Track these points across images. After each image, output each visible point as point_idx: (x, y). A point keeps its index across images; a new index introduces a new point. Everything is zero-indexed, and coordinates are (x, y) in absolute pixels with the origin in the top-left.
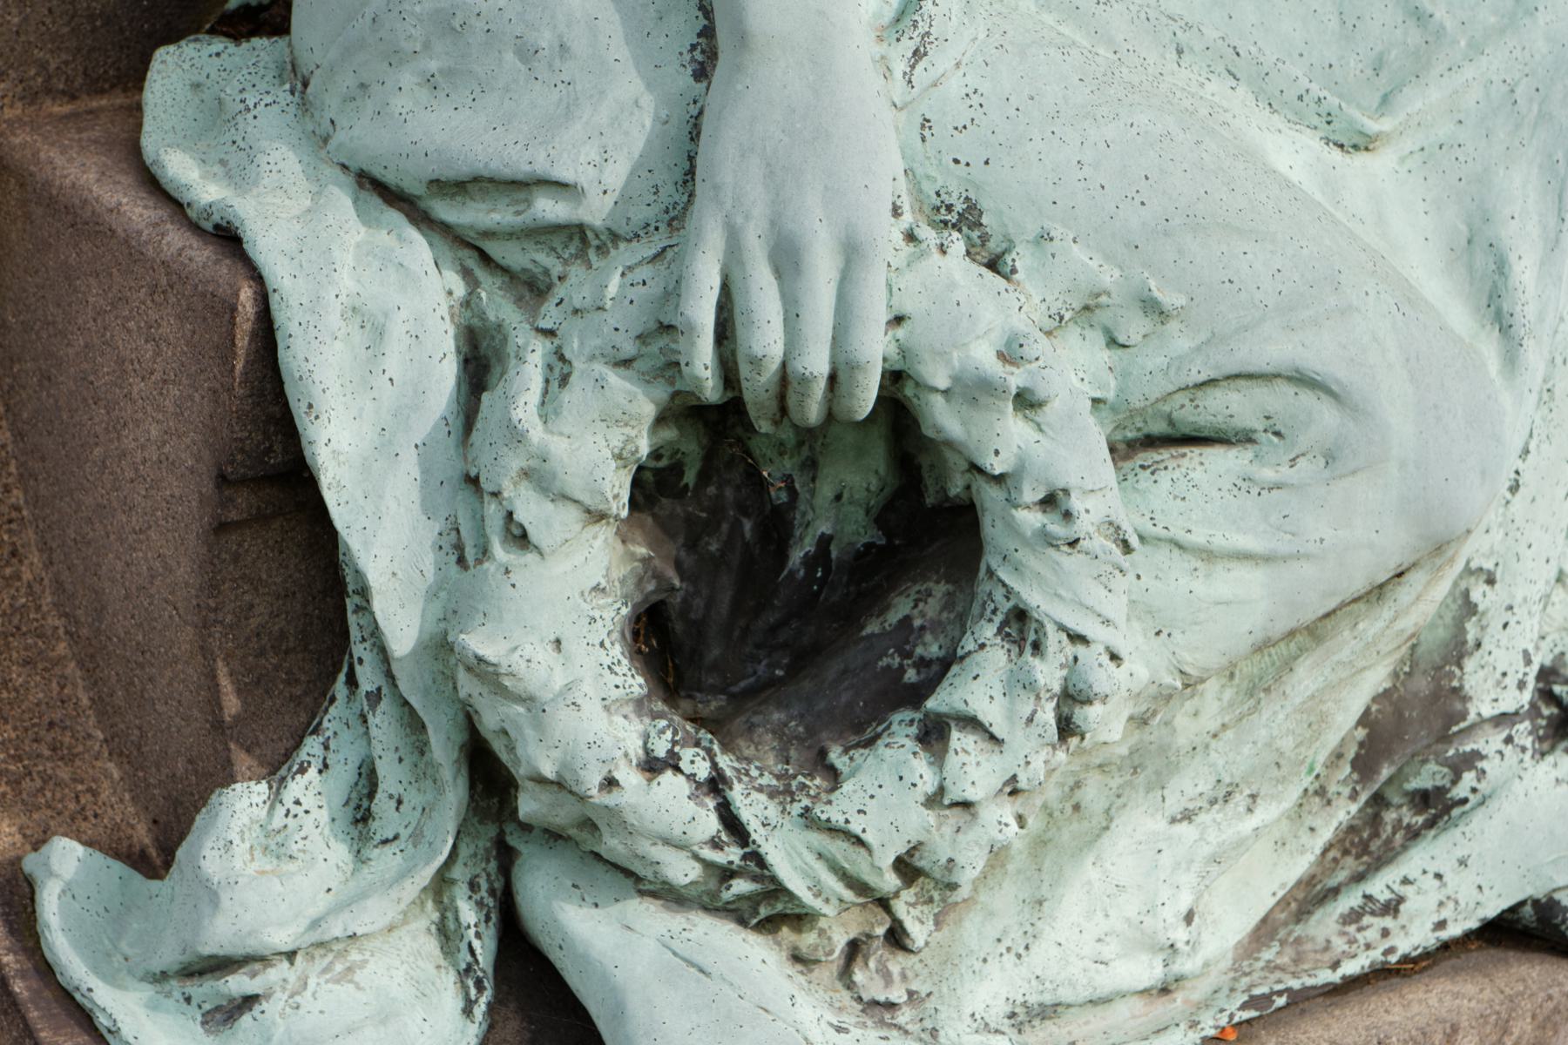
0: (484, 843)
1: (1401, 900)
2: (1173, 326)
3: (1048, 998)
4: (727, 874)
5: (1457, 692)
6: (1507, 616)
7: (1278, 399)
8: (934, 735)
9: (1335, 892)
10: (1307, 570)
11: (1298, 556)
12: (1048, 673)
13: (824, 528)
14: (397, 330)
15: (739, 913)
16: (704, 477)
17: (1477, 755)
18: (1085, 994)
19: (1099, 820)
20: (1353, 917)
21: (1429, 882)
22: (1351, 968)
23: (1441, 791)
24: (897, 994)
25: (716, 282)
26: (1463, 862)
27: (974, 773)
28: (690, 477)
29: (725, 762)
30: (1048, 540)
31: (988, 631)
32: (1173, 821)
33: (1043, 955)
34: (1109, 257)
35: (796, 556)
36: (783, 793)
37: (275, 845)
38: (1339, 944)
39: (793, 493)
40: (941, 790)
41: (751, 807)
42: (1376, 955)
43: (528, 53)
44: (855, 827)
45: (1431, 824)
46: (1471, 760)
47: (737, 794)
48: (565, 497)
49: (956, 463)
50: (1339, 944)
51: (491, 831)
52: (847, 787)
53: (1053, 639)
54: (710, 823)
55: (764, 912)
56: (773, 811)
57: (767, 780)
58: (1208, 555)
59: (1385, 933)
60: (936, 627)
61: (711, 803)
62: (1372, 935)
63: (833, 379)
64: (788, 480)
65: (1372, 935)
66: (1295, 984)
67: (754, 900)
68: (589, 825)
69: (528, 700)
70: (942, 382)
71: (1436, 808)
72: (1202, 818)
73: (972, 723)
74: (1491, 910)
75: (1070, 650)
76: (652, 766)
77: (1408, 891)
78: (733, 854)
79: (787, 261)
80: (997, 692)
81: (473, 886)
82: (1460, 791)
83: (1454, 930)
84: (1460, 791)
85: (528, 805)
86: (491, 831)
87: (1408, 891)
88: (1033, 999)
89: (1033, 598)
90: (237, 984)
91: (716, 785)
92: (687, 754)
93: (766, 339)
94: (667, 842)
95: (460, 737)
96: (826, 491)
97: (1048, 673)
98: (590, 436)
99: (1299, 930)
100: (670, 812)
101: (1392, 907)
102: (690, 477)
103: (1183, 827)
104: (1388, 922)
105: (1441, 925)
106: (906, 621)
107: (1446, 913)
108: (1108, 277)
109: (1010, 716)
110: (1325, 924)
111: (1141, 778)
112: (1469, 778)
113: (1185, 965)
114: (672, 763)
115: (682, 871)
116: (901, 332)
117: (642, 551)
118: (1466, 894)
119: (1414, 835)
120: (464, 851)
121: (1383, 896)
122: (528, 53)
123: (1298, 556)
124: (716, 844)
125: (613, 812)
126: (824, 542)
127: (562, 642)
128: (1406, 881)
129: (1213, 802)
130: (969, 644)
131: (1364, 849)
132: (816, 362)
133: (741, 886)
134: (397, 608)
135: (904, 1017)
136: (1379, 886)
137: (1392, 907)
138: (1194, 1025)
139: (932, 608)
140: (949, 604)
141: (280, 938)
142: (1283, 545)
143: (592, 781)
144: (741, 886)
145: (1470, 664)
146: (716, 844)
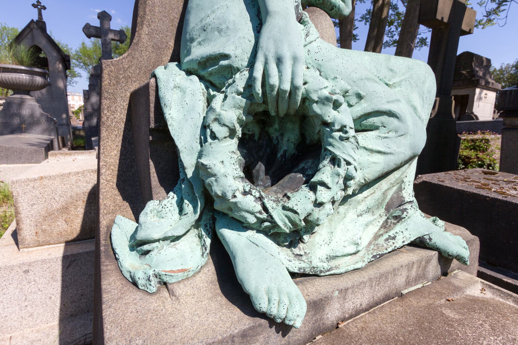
0: (209, 217)
1: (396, 237)
2: (363, 101)
3: (334, 255)
4: (263, 221)
5: (402, 196)
6: (409, 183)
7: (384, 119)
8: (313, 188)
9: (382, 235)
10: (391, 157)
11: (390, 153)
12: (342, 171)
13: (285, 148)
14: (188, 91)
15: (265, 232)
16: (259, 138)
17: (406, 209)
18: (341, 254)
19: (343, 215)
20: (387, 240)
21: (400, 233)
22: (390, 250)
23: (400, 216)
24: (302, 253)
25: (262, 70)
26: (406, 229)
27: (324, 196)
28: (256, 138)
29: (262, 194)
30: (341, 139)
31: (326, 162)
32: (358, 216)
33: (333, 245)
34: (349, 84)
35: (279, 155)
36: (277, 201)
37: (159, 214)
38: (385, 245)
39: (278, 141)
40: (316, 200)
41: (269, 204)
42: (393, 247)
43: (220, 31)
44: (295, 208)
45: (398, 222)
46: (405, 210)
47: (266, 201)
48: (224, 125)
49: (318, 123)
50: (385, 245)
51: (211, 214)
52: (293, 199)
53: (343, 163)
54: (259, 208)
55: (272, 231)
56: (274, 205)
57: (273, 198)
58: (372, 151)
59: (393, 243)
60: (310, 168)
61: (259, 203)
62: (391, 243)
63: (290, 93)
64: (277, 139)
65: (391, 243)
66: (380, 253)
67: (269, 228)
68: (231, 209)
69: (214, 175)
70: (316, 99)
71: (398, 219)
72: (364, 216)
73: (323, 184)
74: (412, 239)
75: (346, 167)
76: (245, 193)
77: (397, 235)
78: (264, 216)
79: (279, 61)
80: (329, 176)
81: (206, 226)
82: (404, 216)
83: (406, 243)
84: (404, 216)
85: (218, 206)
86: (211, 214)
87: (397, 235)
88: (331, 255)
89: (337, 152)
90: (146, 247)
91: (261, 198)
92: (253, 191)
93: (274, 80)
94: (248, 212)
95: (201, 189)
96: (285, 139)
97: (342, 171)
98: (230, 110)
99: (376, 242)
100: (249, 203)
101: (394, 238)
102: (256, 138)
103: (360, 218)
104: (393, 241)
105: (404, 242)
106: (303, 168)
107: (404, 239)
108: (349, 88)
109: (333, 181)
110: (381, 241)
111: (351, 207)
112: (405, 213)
113: (360, 248)
114: (249, 193)
115: (252, 220)
116: (306, 86)
117: (245, 151)
118: (408, 236)
119: (395, 224)
120: (204, 218)
121: (393, 236)
122: (220, 31)
123: (390, 153)
124: (260, 213)
125: (235, 203)
126: (285, 151)
127: (225, 164)
128: (396, 233)
129: (366, 213)
130: (321, 166)
131: (385, 227)
132: (287, 87)
133: (267, 224)
134: (189, 161)
135: (304, 258)
136: (391, 233)
137: (394, 238)
138: (364, 261)
139: (309, 164)
140: (313, 163)
141: (156, 236)
142: (388, 151)
143: (229, 195)
144: (267, 224)
145: (403, 192)
146: (260, 213)
